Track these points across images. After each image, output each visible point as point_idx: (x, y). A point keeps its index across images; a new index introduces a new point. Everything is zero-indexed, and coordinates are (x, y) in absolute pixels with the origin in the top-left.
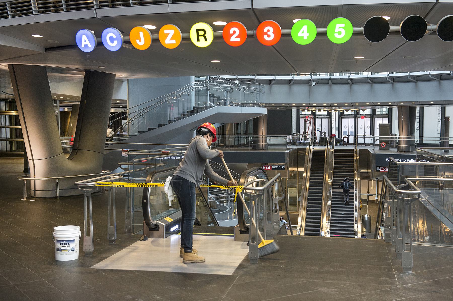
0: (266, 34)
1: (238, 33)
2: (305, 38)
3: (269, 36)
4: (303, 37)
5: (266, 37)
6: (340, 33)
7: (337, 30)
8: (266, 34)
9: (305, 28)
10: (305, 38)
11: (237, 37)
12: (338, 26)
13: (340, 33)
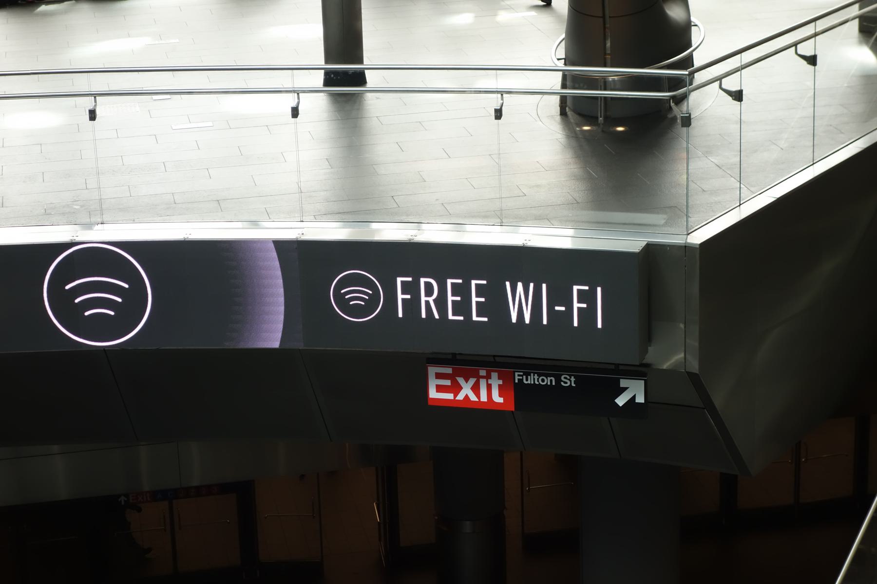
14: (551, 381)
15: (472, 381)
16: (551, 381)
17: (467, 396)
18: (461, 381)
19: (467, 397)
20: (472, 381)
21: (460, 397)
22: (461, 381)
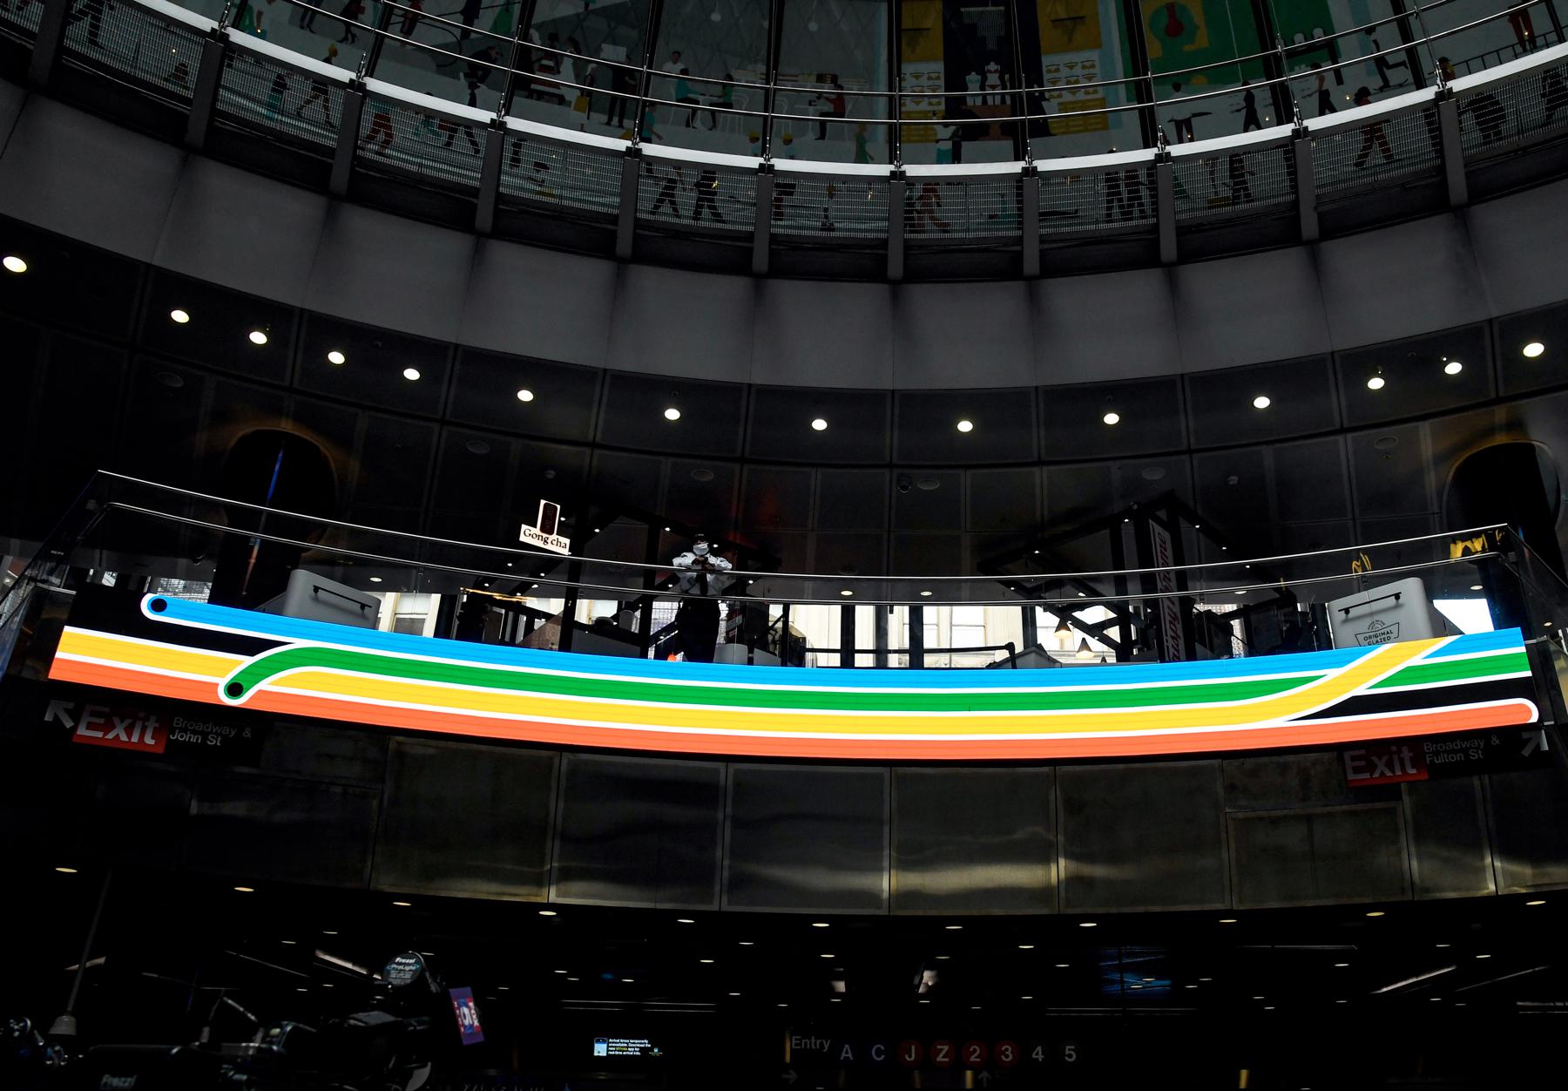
1: (978, 1052)
2: (1040, 1060)
4: (1038, 1059)
5: (1003, 1057)
6: (1070, 1056)
7: (1067, 1052)
8: (1003, 1053)
9: (1039, 1049)
10: (1040, 1060)
11: (976, 1057)
12: (1068, 1047)
13: (1070, 1056)
14: (1460, 756)
15: (1385, 759)
16: (1460, 756)
17: (1382, 774)
18: (1375, 759)
19: (1382, 774)
20: (1385, 759)
21: (1376, 775)
22: (1375, 759)
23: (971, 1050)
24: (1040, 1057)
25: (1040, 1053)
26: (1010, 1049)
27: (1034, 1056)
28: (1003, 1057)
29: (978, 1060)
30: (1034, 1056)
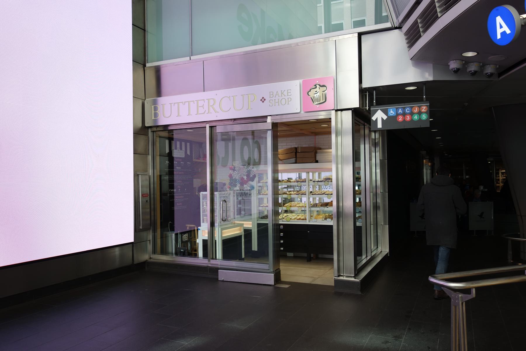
0: (407, 118)
1: (401, 118)
3: (408, 118)
5: (407, 119)
6: (424, 117)
7: (423, 116)
8: (407, 118)
9: (416, 116)
10: (416, 118)
12: (423, 115)
13: (424, 117)
23: (399, 117)
24: (416, 118)
25: (416, 117)
26: (409, 117)
27: (415, 118)
28: (407, 119)
29: (401, 120)
30: (415, 118)
